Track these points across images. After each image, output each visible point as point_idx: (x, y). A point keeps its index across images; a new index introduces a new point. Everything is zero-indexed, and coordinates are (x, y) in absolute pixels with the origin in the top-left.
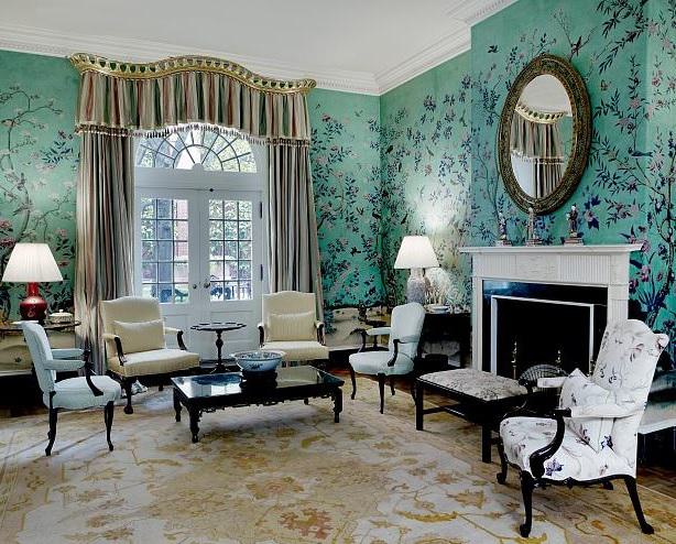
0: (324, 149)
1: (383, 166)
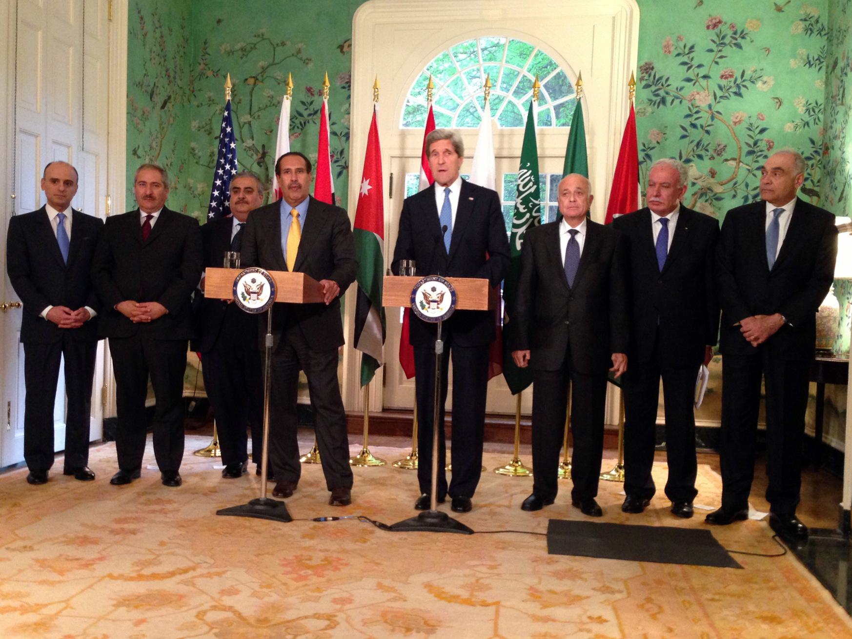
0: (706, 77)
1: (827, 98)
